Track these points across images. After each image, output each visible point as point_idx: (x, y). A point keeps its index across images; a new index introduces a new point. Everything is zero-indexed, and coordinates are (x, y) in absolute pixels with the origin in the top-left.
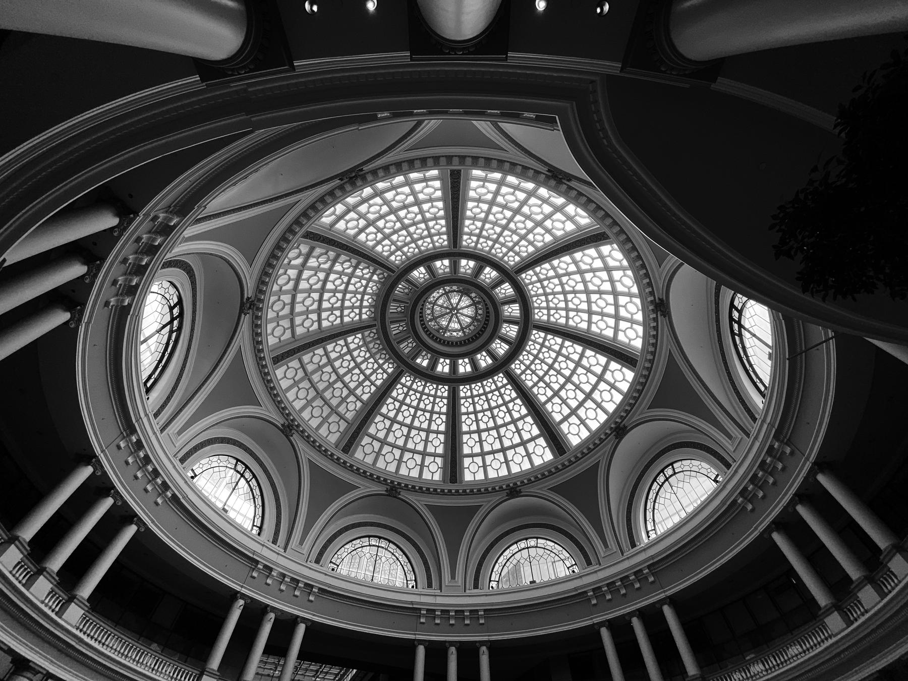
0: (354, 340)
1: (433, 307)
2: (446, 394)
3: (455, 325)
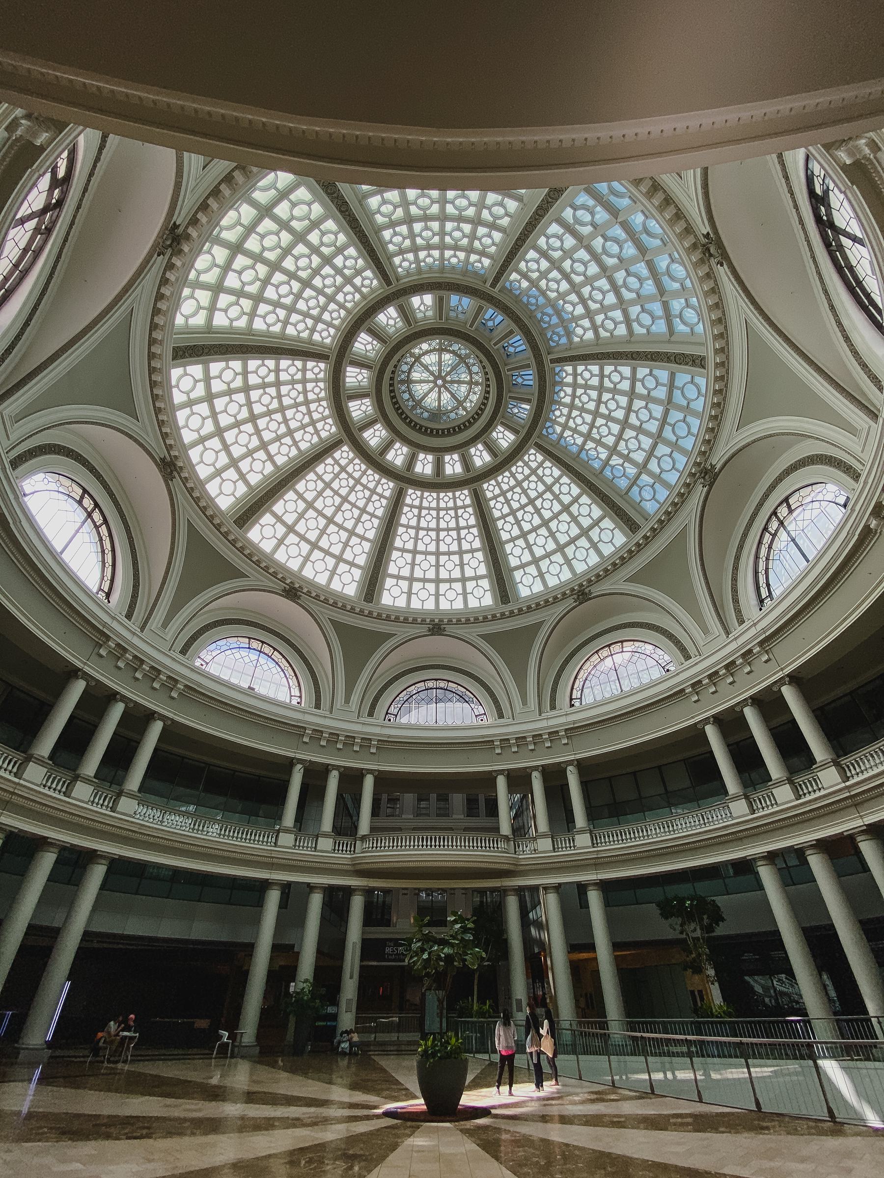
0: (583, 333)
1: (471, 378)
3: (430, 359)
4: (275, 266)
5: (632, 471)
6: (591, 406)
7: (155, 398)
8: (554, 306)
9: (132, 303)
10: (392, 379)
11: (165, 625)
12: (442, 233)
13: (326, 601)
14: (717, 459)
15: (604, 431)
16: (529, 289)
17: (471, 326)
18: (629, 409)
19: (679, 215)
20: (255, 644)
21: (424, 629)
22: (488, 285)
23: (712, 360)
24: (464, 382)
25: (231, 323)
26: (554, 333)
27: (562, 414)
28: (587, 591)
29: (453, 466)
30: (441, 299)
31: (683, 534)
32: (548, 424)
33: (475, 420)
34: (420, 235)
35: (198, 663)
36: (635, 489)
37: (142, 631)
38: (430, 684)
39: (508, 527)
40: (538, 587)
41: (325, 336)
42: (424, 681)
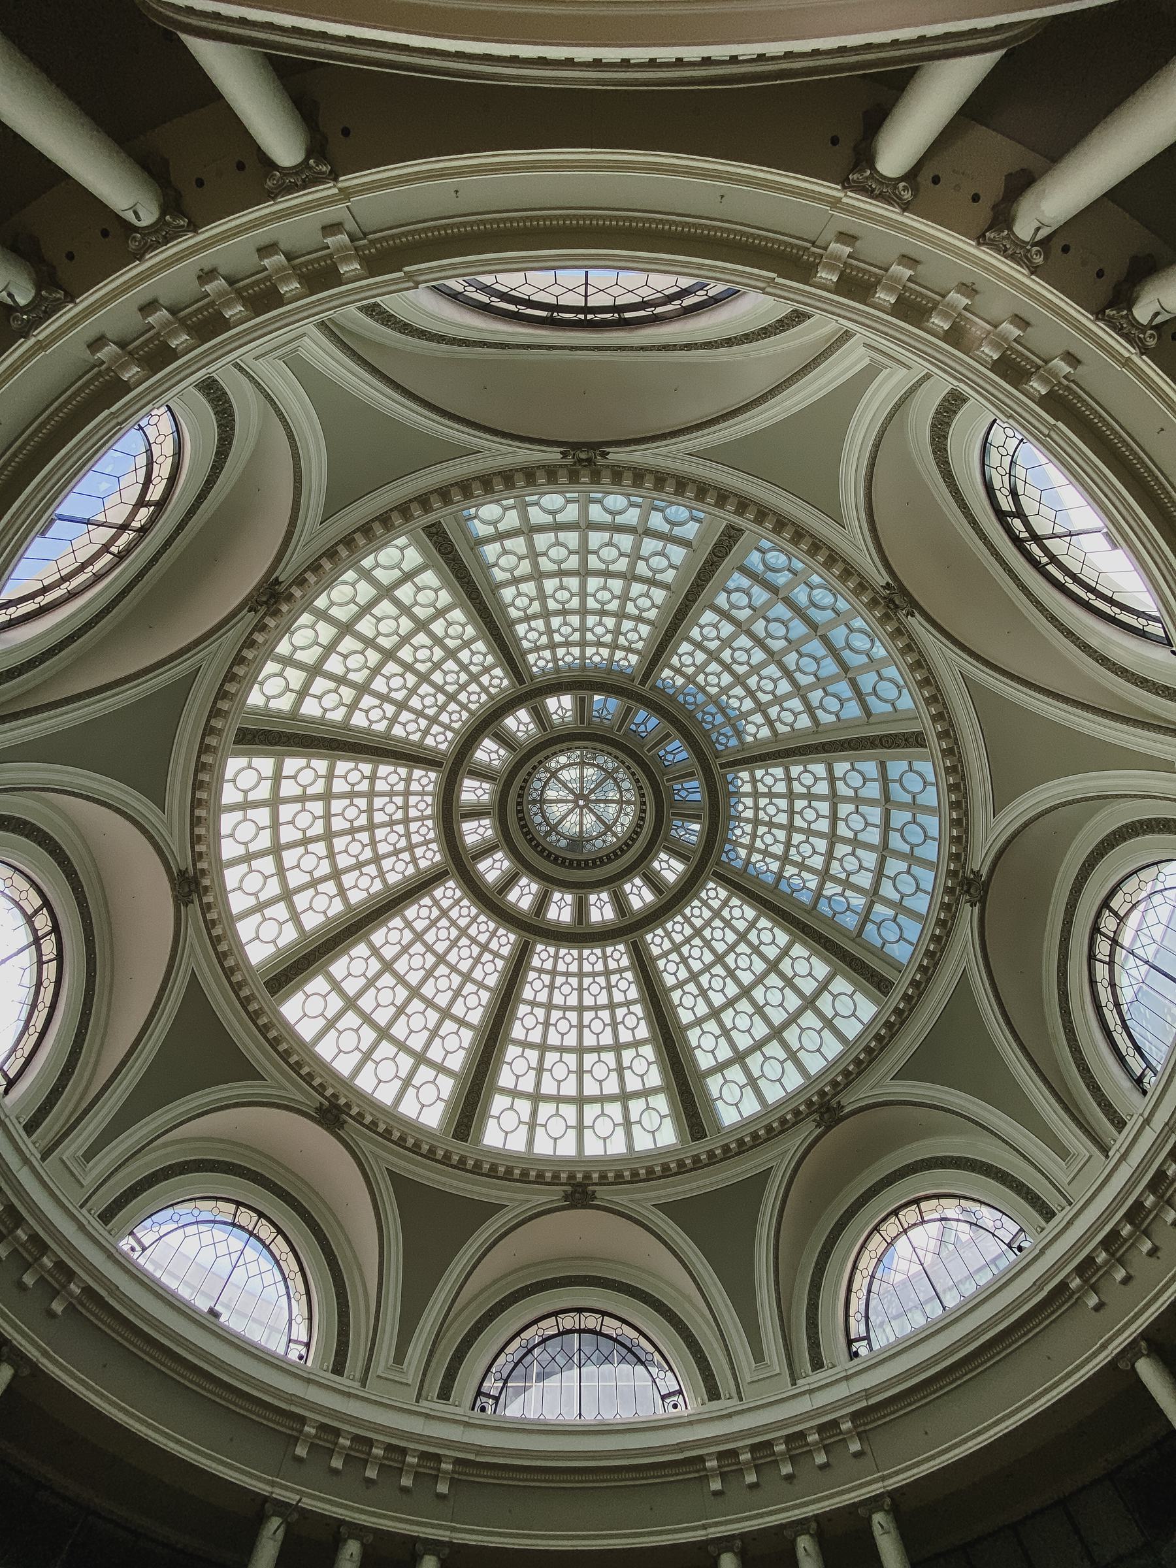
0: (756, 730)
1: (621, 796)
2: (532, 658)
4: (389, 655)
5: (858, 901)
6: (782, 819)
7: (198, 785)
8: (716, 703)
9: (203, 659)
10: (520, 796)
11: (89, 1155)
12: (583, 629)
13: (387, 1134)
14: (980, 859)
15: (806, 849)
16: (684, 686)
17: (619, 730)
18: (834, 818)
19: (848, 572)
20: (246, 1218)
21: (553, 1195)
22: (637, 683)
23: (931, 731)
24: (612, 802)
25: (324, 714)
26: (720, 734)
27: (746, 808)
28: (834, 1103)
29: (601, 910)
30: (582, 700)
31: (963, 982)
32: (728, 847)
33: (629, 846)
34: (558, 631)
35: (126, 1244)
36: (870, 927)
37: (43, 1159)
38: (568, 1322)
39: (688, 1001)
40: (751, 1107)
41: (440, 741)
42: (556, 1314)
